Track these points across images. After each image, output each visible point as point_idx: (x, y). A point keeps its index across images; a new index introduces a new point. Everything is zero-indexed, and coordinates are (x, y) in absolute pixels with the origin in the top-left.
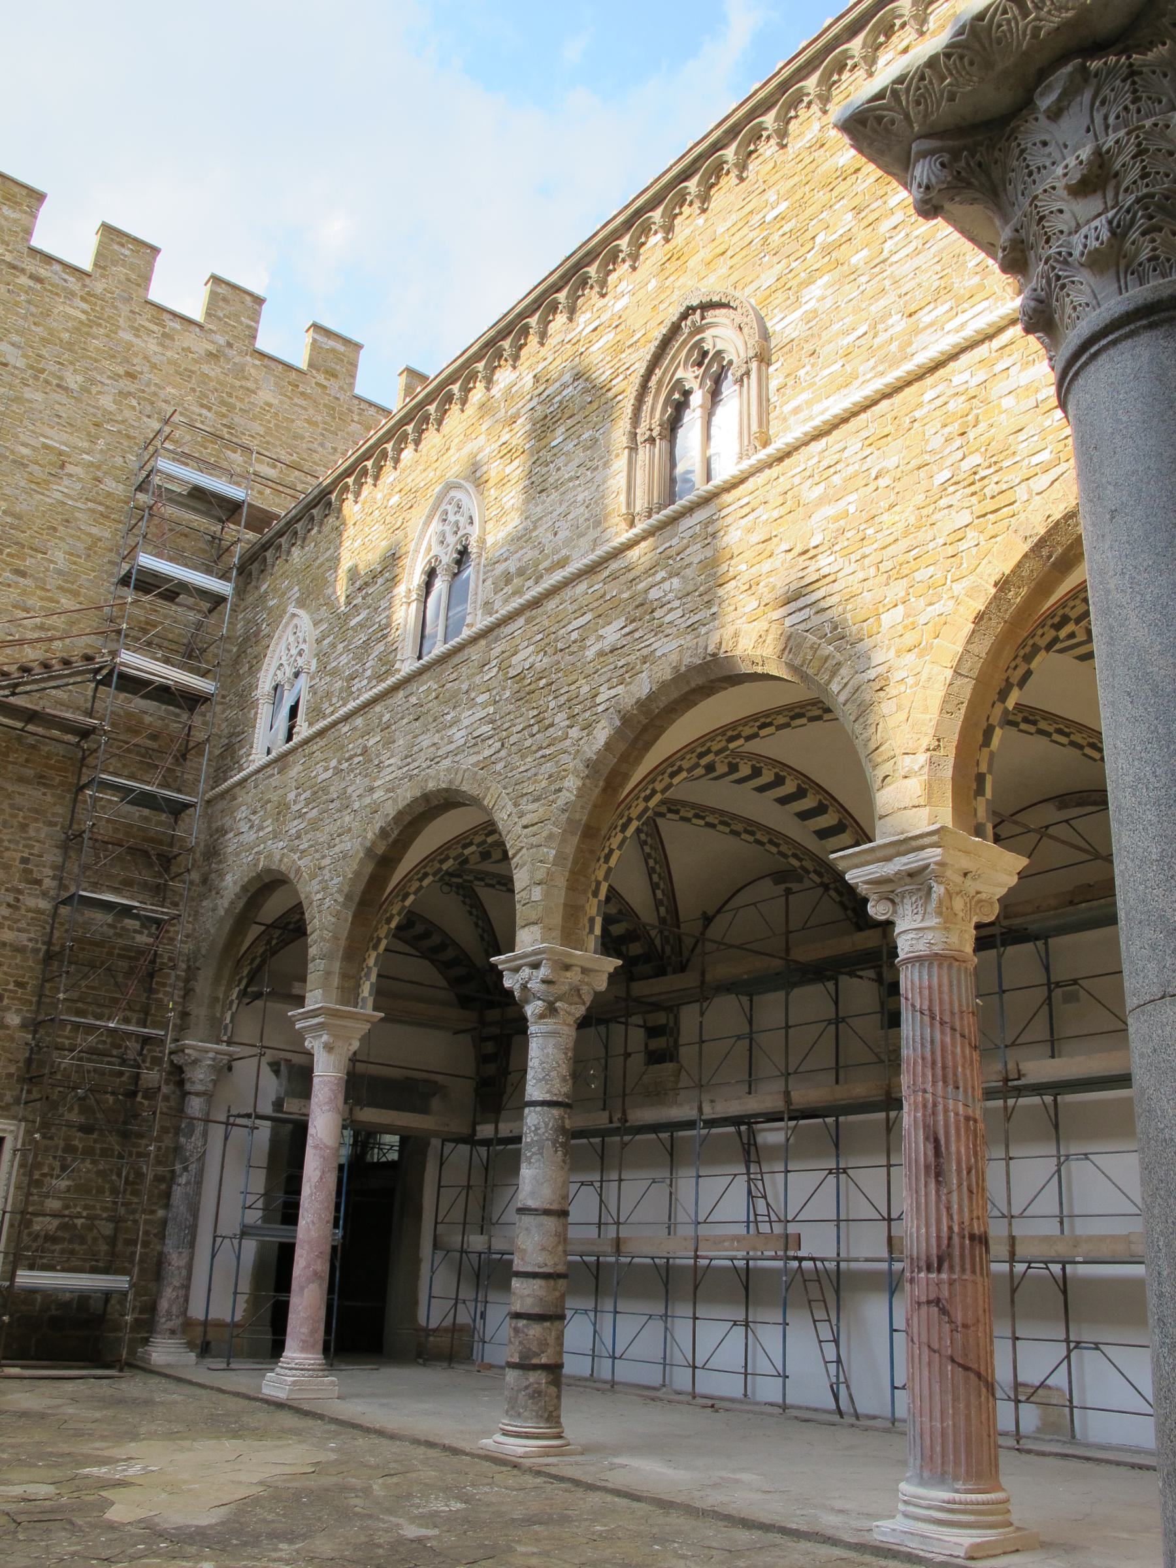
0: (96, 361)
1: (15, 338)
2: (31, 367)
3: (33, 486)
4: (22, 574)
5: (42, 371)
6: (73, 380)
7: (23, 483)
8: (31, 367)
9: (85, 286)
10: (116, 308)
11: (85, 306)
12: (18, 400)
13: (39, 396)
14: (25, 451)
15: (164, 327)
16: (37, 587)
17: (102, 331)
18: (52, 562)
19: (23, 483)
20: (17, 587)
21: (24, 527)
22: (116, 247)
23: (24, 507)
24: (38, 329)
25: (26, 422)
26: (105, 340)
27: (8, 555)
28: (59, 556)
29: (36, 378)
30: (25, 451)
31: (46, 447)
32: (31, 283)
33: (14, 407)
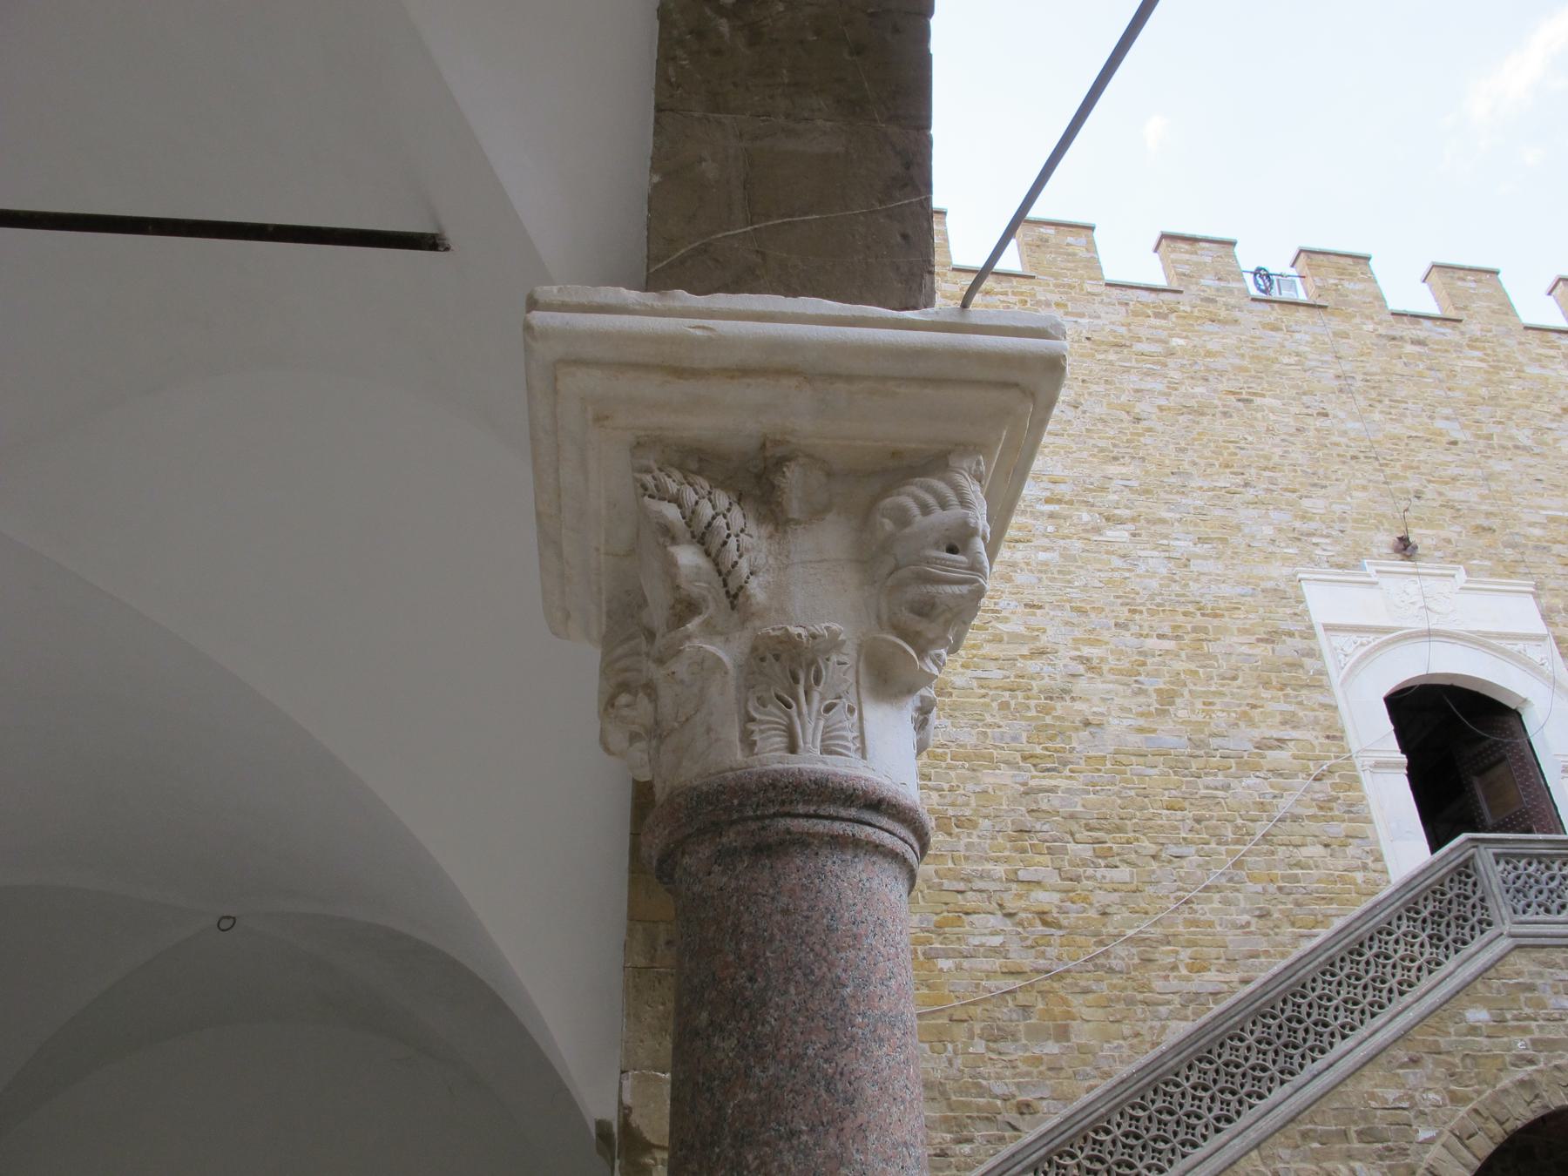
0: (1528, 407)
1: (1447, 411)
2: (1478, 437)
5: (1489, 437)
6: (1524, 437)
8: (1478, 437)
9: (1462, 333)
10: (1503, 345)
11: (1476, 353)
12: (1488, 478)
13: (1505, 466)
14: (1537, 532)
15: (1559, 348)
17: (1511, 374)
22: (1460, 283)
24: (1457, 394)
25: (1515, 498)
26: (1520, 382)
29: (1491, 447)
30: (1537, 532)
31: (1552, 519)
32: (1417, 349)
33: (1493, 485)
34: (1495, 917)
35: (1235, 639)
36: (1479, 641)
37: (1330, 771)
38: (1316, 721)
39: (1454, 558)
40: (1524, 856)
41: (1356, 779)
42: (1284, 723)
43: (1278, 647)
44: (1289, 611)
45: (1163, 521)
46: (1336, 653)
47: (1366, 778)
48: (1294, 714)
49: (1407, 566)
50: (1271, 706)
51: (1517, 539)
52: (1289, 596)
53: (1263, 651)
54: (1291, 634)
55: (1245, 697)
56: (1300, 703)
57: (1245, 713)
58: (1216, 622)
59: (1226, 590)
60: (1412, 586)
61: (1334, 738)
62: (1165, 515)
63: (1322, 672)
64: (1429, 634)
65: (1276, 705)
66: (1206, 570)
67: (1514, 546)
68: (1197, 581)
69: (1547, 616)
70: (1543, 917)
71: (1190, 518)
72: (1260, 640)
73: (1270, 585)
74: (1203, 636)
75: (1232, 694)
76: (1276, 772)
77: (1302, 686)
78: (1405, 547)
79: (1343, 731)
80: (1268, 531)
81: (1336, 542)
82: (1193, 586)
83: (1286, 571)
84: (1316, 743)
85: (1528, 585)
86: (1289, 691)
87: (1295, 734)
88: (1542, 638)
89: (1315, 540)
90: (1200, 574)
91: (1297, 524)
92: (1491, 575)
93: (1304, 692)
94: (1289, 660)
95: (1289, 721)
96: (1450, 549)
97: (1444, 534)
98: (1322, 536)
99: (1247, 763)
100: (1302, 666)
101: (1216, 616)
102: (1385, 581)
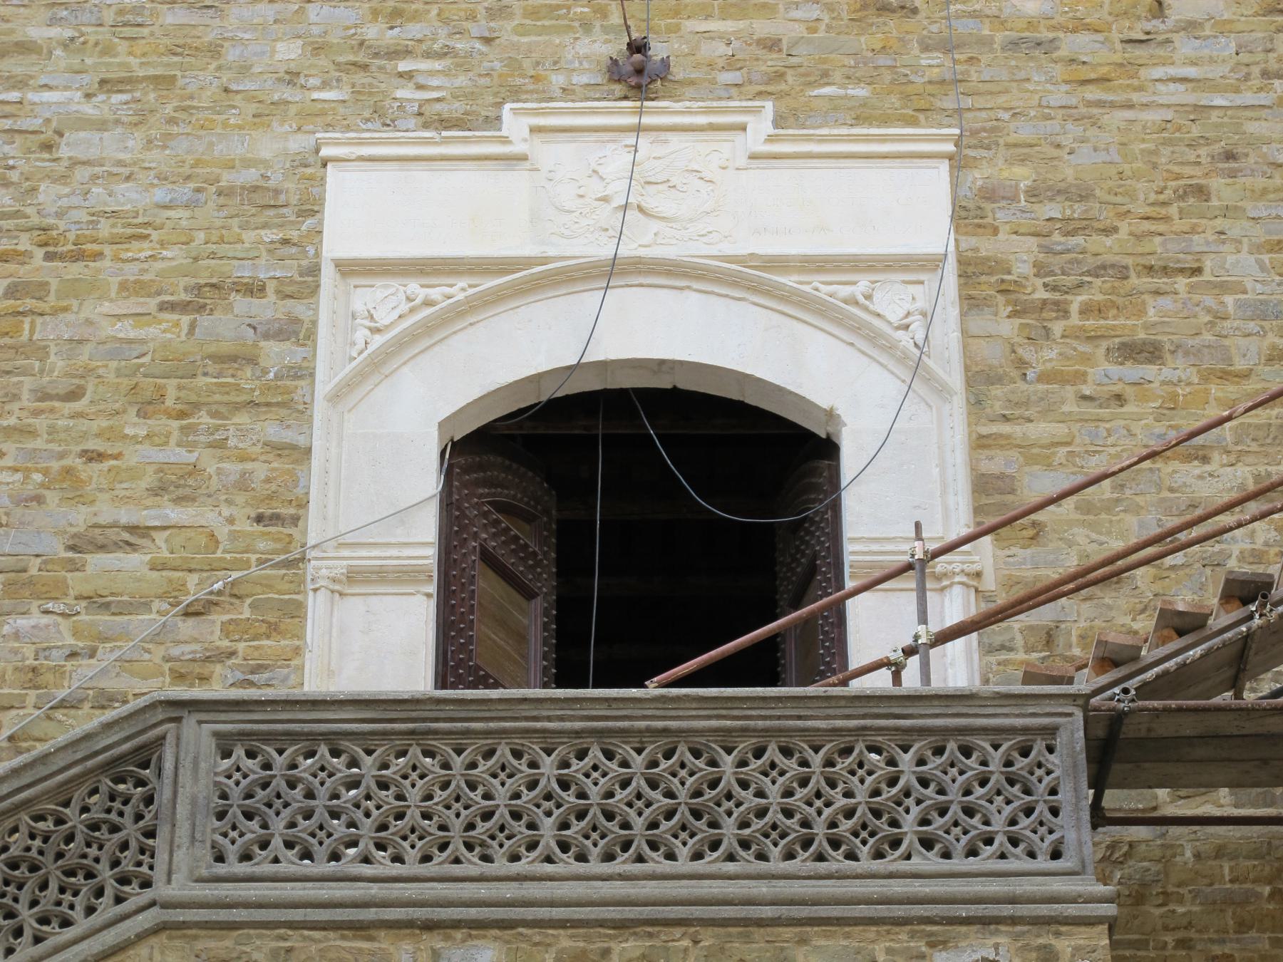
3: (1092, 93)
4: (1148, 352)
7: (1059, 96)
16: (1206, 377)
18: (1223, 288)
19: (1059, 96)
20: (1144, 398)
21: (1106, 216)
23: (1085, 156)
27: (1085, 311)
28: (1242, 264)
34: (158, 875)
35: (107, 307)
36: (752, 279)
37: (235, 593)
38: (243, 484)
39: (768, 86)
40: (293, 737)
41: (296, 611)
42: (158, 491)
43: (204, 320)
44: (269, 235)
45: (25, 48)
46: (347, 322)
47: (316, 605)
48: (194, 469)
49: (622, 113)
50: (133, 456)
51: (965, 27)
52: (294, 205)
53: (166, 332)
54: (254, 289)
55: (84, 436)
56: (221, 445)
57: (68, 471)
58: (74, 270)
59: (128, 196)
60: (615, 159)
61: (276, 519)
62: (37, 33)
63: (304, 372)
64: (612, 272)
65: (150, 448)
66: (93, 153)
67: (948, 46)
68: (63, 179)
69: (966, 216)
70: (291, 863)
71: (92, 34)
72: (163, 307)
73: (250, 176)
74: (29, 303)
75: (52, 430)
76: (98, 602)
77: (237, 407)
78: (638, 73)
79: (303, 504)
80: (288, 51)
81: (463, 63)
82: (48, 194)
83: (299, 143)
84: (223, 532)
85: (940, 138)
86: (203, 419)
87: (175, 514)
88: (931, 263)
89: (403, 66)
90: (75, 163)
91: (372, 32)
92: (859, 120)
93: (242, 418)
94: (226, 348)
95: (177, 485)
96: (772, 61)
97: (763, 27)
98: (428, 55)
99: (31, 582)
100: (252, 361)
101: (78, 256)
102: (553, 154)
